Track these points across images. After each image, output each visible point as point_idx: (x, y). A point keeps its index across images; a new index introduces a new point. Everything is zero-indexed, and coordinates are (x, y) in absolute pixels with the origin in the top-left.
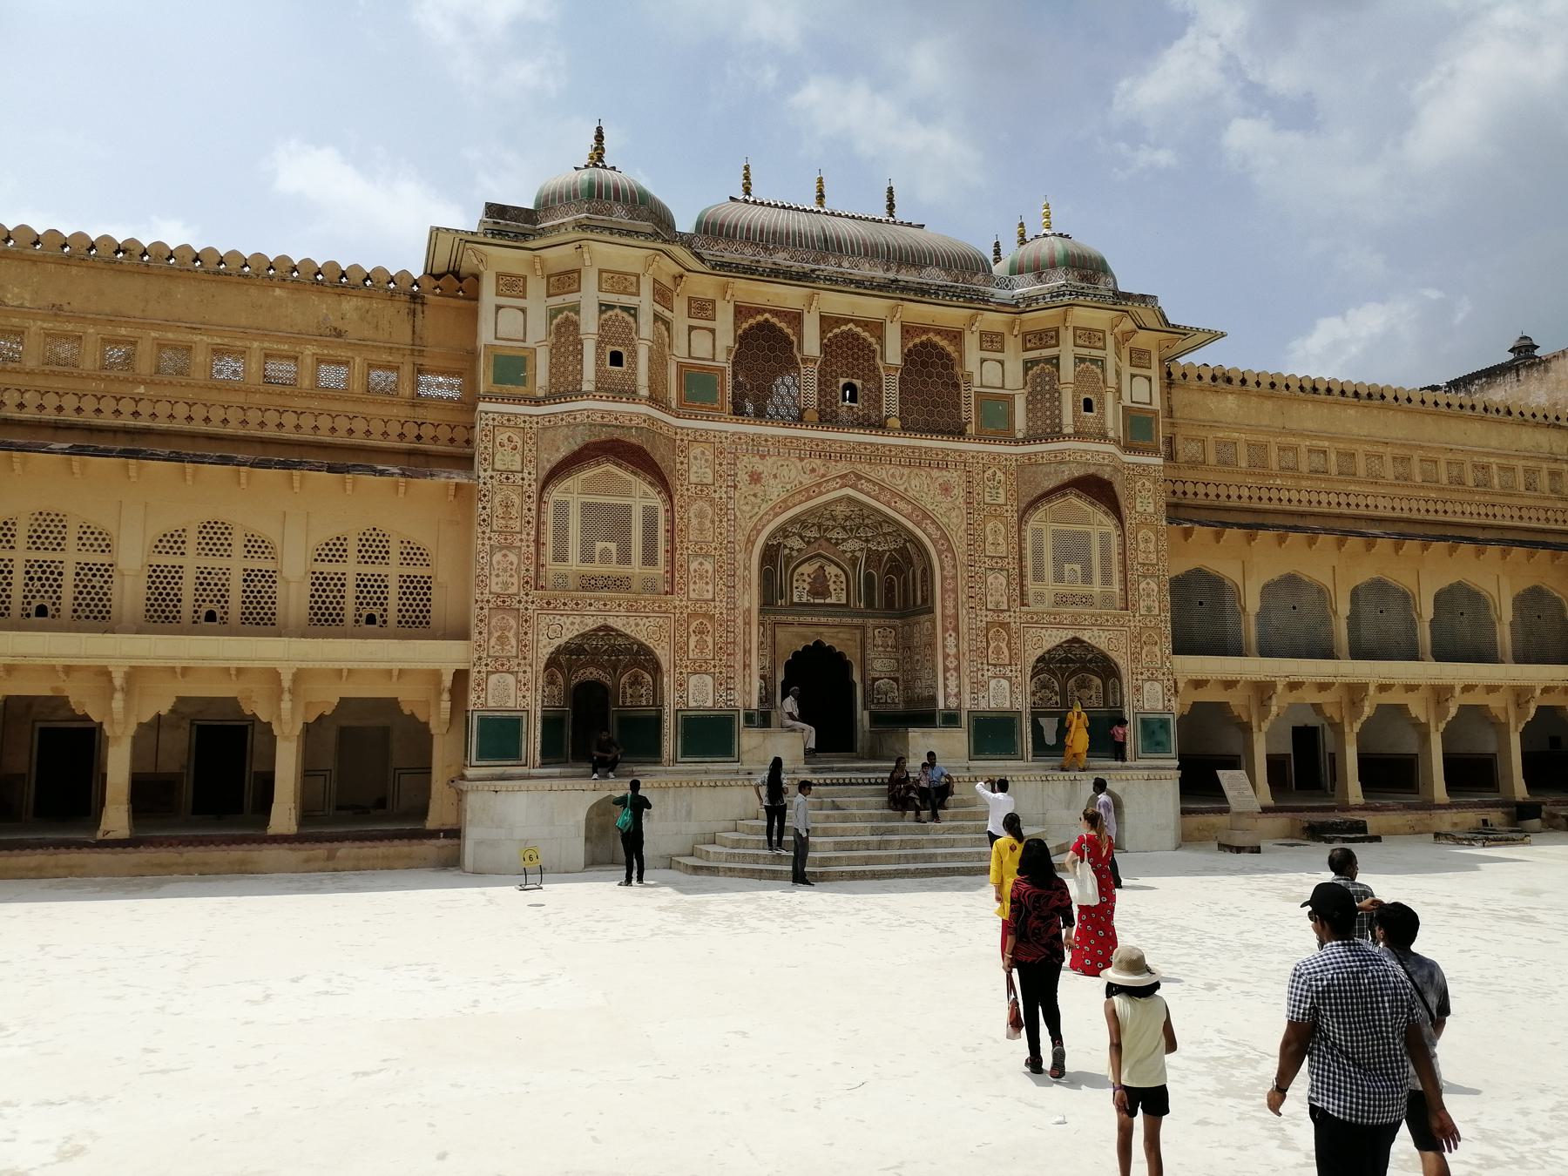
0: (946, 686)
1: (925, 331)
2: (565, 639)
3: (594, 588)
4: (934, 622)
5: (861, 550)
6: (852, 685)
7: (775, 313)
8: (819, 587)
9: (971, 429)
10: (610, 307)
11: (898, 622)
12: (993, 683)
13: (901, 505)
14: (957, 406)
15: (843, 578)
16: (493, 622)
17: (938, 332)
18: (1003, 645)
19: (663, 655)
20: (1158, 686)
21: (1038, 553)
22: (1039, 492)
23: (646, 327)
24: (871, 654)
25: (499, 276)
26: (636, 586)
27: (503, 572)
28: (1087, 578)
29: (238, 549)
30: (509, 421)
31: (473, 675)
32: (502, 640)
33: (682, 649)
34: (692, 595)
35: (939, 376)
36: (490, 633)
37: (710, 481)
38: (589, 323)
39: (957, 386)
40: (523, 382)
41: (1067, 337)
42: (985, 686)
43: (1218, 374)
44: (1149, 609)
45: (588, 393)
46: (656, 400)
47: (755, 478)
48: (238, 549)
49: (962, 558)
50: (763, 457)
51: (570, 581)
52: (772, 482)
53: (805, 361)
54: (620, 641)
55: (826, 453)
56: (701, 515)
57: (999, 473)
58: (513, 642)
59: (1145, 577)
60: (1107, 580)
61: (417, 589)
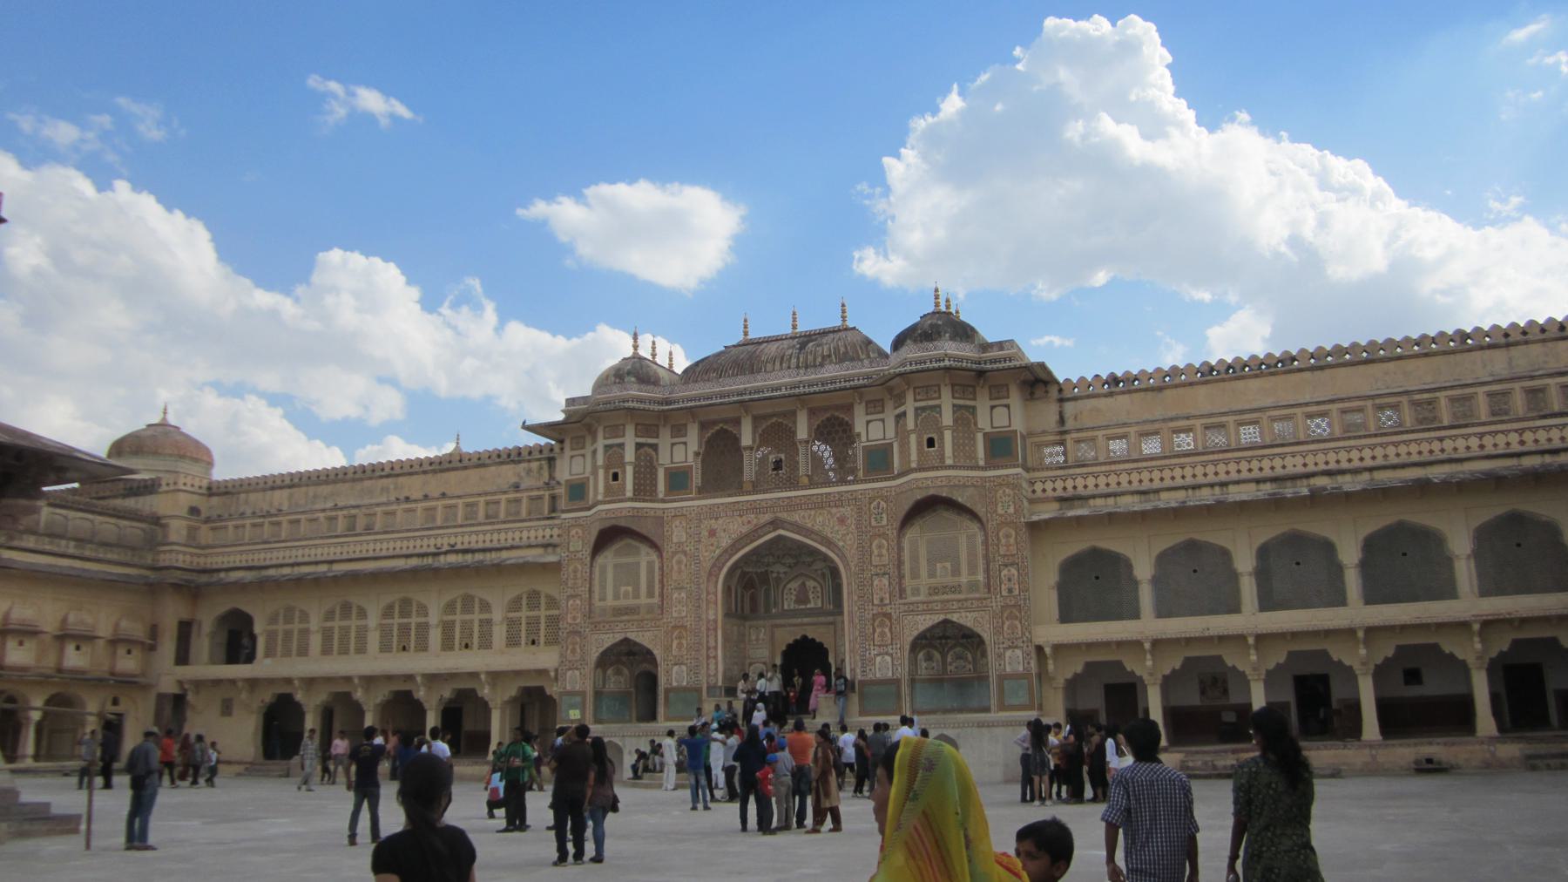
1: (826, 409)
7: (726, 421)
8: (802, 598)
12: (878, 659)
17: (837, 408)
20: (1018, 652)
21: (915, 558)
28: (956, 571)
29: (477, 608)
30: (576, 523)
32: (573, 651)
33: (668, 648)
41: (910, 397)
42: (872, 662)
44: (1010, 591)
47: (712, 533)
48: (477, 608)
53: (746, 448)
55: (755, 508)
56: (679, 562)
60: (973, 569)
61: (553, 621)
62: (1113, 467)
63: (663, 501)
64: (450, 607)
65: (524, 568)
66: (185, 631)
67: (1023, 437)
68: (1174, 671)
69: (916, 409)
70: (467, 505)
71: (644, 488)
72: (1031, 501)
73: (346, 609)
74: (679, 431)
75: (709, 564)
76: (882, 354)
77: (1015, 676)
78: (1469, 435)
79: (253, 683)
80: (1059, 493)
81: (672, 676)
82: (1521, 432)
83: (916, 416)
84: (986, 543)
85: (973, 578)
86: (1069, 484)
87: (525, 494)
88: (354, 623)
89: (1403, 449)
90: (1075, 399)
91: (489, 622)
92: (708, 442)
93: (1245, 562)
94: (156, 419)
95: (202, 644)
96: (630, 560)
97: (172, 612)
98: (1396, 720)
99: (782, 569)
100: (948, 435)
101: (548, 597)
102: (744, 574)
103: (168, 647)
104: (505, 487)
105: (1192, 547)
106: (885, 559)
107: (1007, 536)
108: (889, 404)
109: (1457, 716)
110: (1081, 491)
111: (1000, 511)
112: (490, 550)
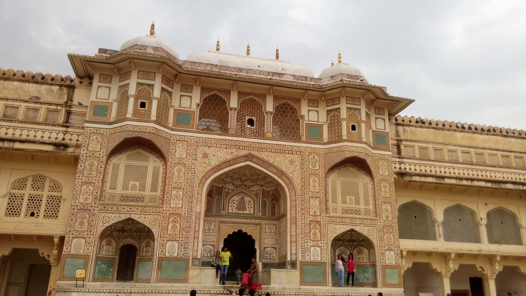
0: (291, 250)
1: (284, 98)
2: (110, 224)
3: (127, 201)
4: (286, 220)
5: (260, 190)
6: (255, 250)
7: (219, 91)
8: (241, 206)
9: (304, 138)
10: (142, 84)
11: (277, 222)
12: (312, 249)
13: (272, 169)
14: (298, 128)
15: (252, 202)
16: (78, 215)
18: (318, 231)
19: (156, 231)
20: (392, 253)
21: (334, 191)
22: (333, 164)
23: (157, 93)
24: (264, 236)
25: (100, 75)
26: (146, 200)
27: (86, 195)
28: (357, 202)
30: (97, 132)
31: (66, 238)
32: (82, 223)
34: (172, 205)
35: (291, 116)
36: (76, 221)
37: (185, 157)
38: (132, 90)
39: (298, 121)
40: (105, 115)
42: (309, 250)
43: (419, 120)
44: (387, 217)
45: (127, 118)
47: (205, 156)
49: (299, 192)
50: (209, 147)
51: (116, 197)
52: (213, 158)
53: (231, 109)
54: (139, 226)
55: (237, 146)
56: (179, 171)
57: (316, 156)
58: (86, 224)
60: (367, 203)
62: (423, 162)
69: (348, 108)
74: (187, 88)
75: (202, 175)
83: (347, 112)
85: (367, 207)
86: (403, 166)
87: (44, 107)
92: (204, 100)
96: (140, 163)
102: (213, 186)
104: (27, 98)
106: (317, 189)
111: (381, 173)
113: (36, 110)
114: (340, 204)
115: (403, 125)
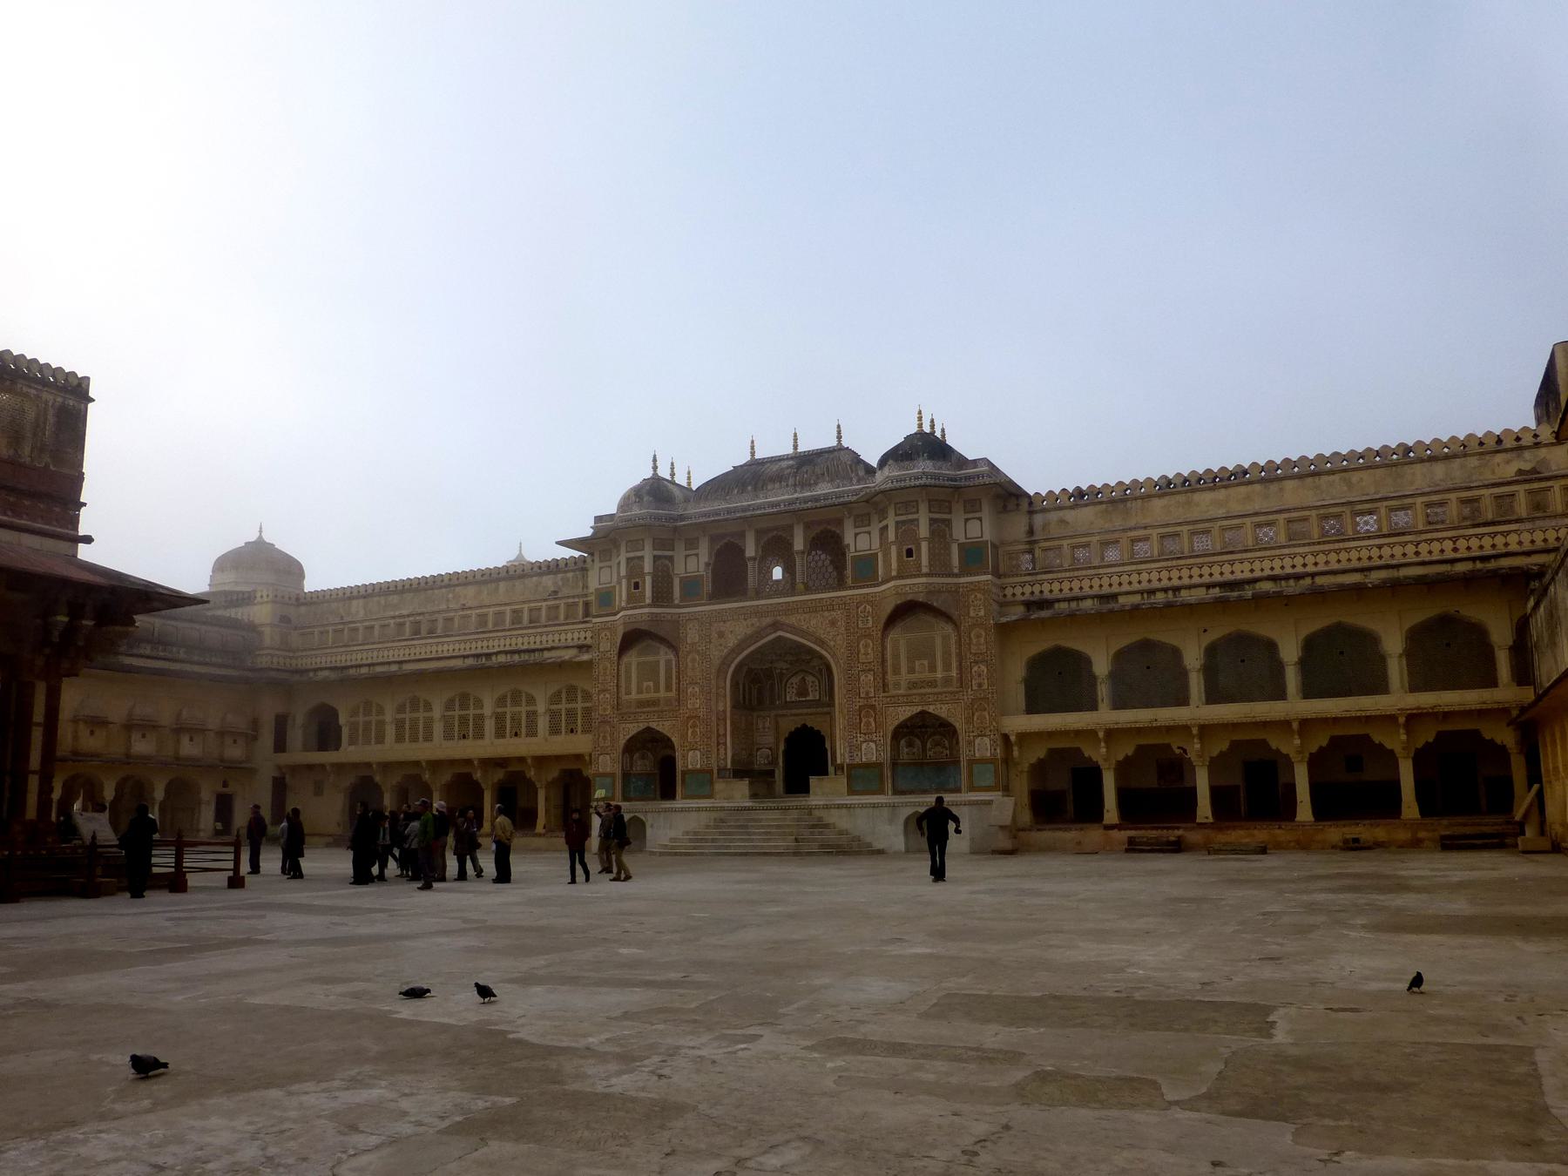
9: (849, 581)
20: (987, 740)
21: (896, 656)
28: (933, 668)
33: (684, 736)
39: (844, 554)
41: (891, 513)
44: (980, 685)
46: (654, 604)
55: (757, 612)
59: (976, 662)
60: (947, 667)
63: (679, 607)
64: (501, 701)
65: (561, 666)
66: (281, 724)
67: (994, 546)
68: (1127, 757)
70: (514, 611)
71: (662, 595)
72: (1002, 605)
73: (415, 705)
74: (692, 544)
76: (870, 470)
77: (982, 761)
78: (1406, 543)
79: (340, 768)
80: (1027, 597)
81: (689, 759)
82: (1454, 539)
83: (897, 529)
84: (959, 643)
86: (1037, 589)
88: (421, 715)
89: (1343, 556)
90: (1044, 510)
91: (535, 713)
93: (1193, 658)
94: (253, 538)
95: (296, 736)
96: (651, 658)
97: (269, 709)
98: (1334, 802)
99: (785, 666)
100: (924, 546)
101: (583, 691)
103: (267, 740)
105: (1146, 646)
106: (871, 657)
107: (978, 636)
108: (875, 518)
109: (1383, 803)
110: (1047, 595)
112: (533, 651)
113: (557, 607)
114: (905, 676)
115: (1044, 510)
